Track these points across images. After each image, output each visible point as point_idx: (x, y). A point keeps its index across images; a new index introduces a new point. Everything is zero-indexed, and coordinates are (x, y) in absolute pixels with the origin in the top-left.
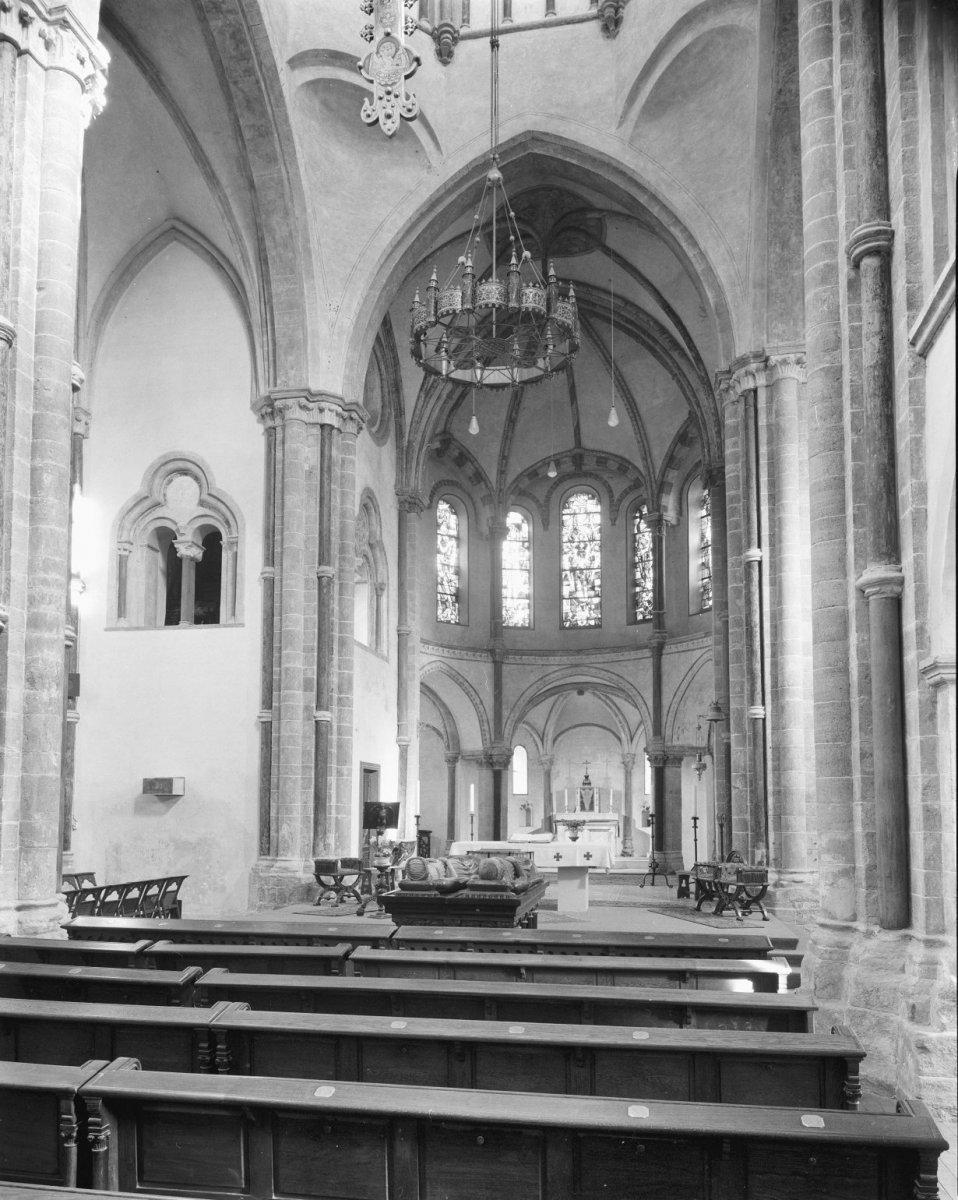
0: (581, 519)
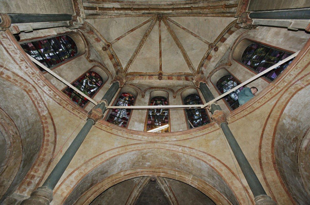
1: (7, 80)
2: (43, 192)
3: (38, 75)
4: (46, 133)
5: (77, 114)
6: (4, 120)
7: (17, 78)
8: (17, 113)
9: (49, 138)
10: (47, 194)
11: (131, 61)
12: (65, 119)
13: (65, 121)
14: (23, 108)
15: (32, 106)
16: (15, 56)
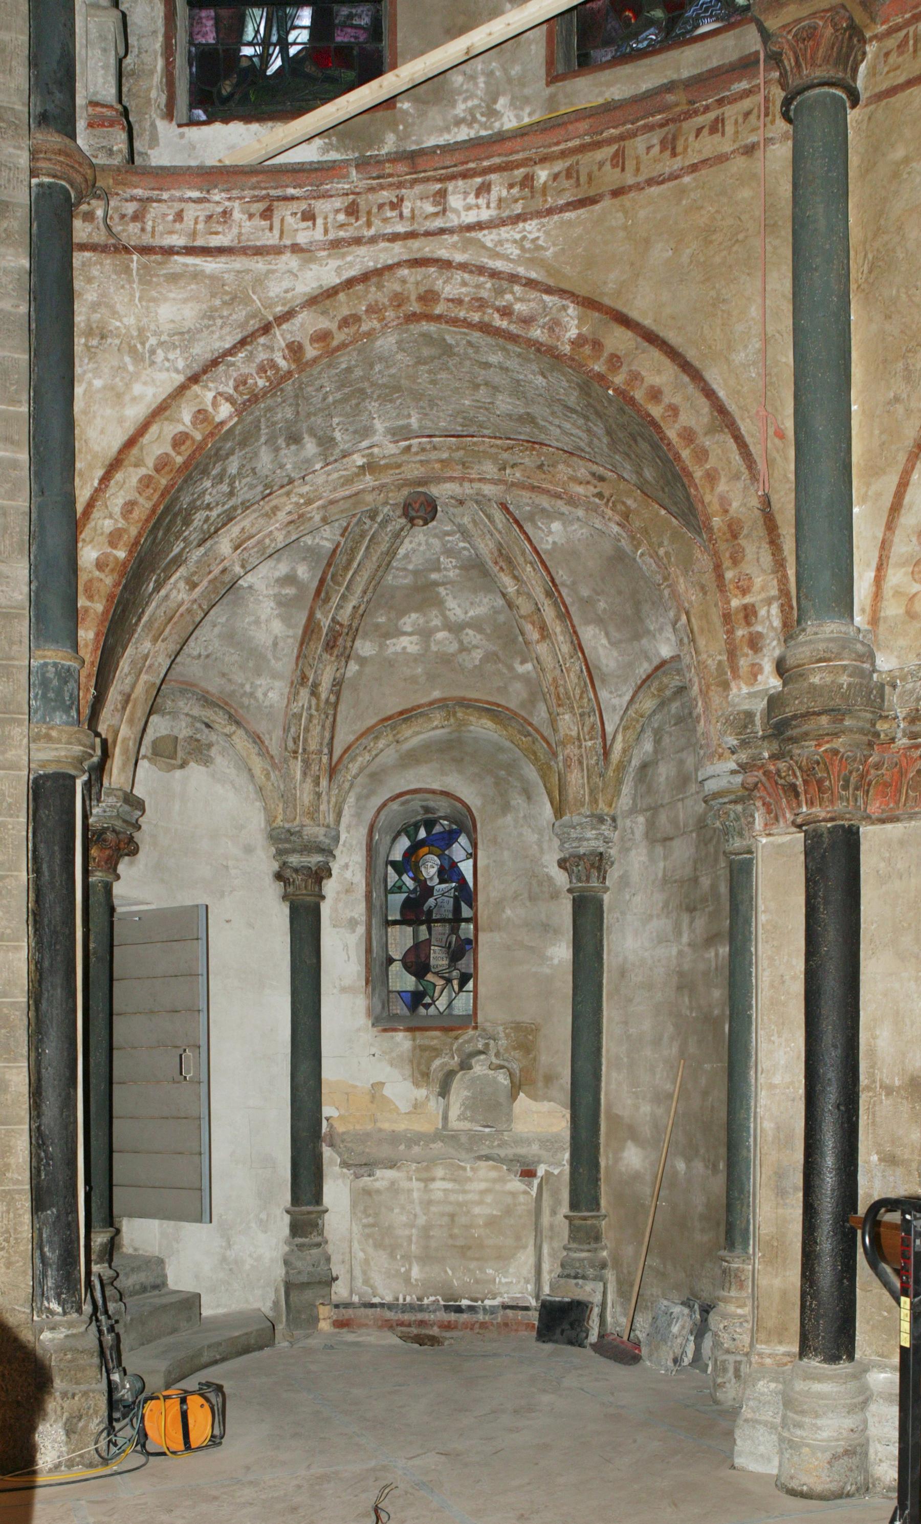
1: (332, 352)
2: (801, 650)
3: (371, 189)
4: (656, 411)
5: (709, 145)
6: (512, 467)
7: (344, 305)
8: (510, 407)
9: (686, 419)
10: (821, 646)
12: (675, 250)
13: (685, 259)
14: (498, 379)
15: (504, 349)
16: (235, 231)
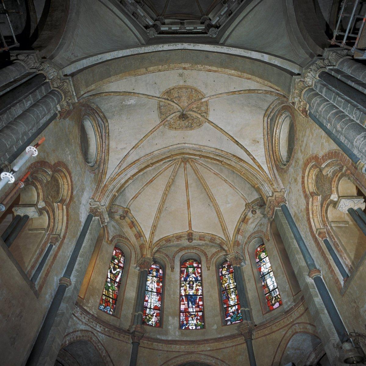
0: (191, 270)
11: (154, 227)
